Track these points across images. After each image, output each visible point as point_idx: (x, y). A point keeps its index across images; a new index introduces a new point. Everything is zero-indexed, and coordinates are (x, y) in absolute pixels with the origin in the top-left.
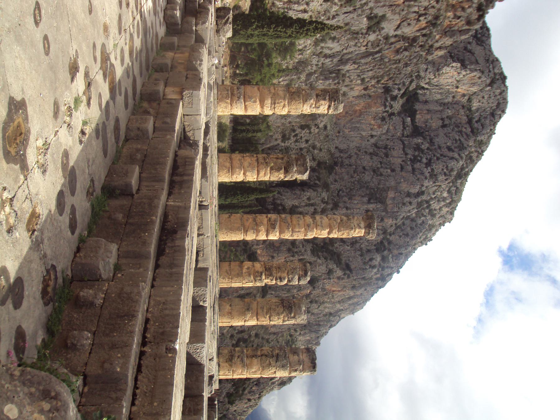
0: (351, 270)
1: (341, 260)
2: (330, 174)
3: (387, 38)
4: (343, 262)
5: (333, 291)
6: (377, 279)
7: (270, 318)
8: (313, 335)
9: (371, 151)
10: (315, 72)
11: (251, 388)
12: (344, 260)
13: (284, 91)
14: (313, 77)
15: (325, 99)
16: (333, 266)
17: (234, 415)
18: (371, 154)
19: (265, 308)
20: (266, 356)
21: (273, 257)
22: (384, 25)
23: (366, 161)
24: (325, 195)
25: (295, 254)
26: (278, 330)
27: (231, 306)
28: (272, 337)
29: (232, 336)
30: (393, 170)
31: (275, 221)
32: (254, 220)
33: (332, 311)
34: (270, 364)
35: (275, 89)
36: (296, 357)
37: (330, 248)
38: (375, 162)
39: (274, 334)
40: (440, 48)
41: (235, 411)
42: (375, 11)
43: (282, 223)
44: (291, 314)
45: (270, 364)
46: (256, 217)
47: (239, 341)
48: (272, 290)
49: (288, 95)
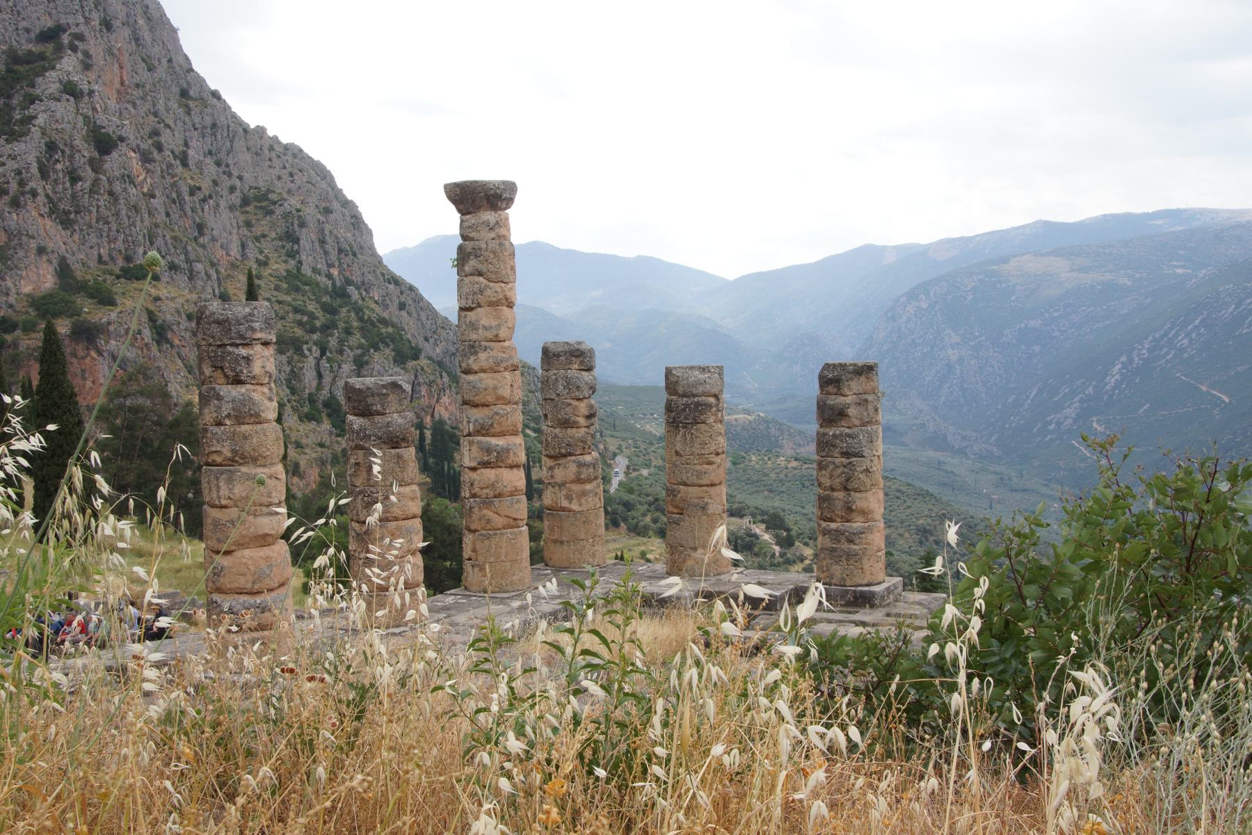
1: (30, 52)
4: (36, 48)
5: (122, 84)
7: (718, 454)
8: (240, 144)
11: (376, 302)
13: (230, 481)
15: (248, 359)
16: (49, 83)
19: (699, 467)
20: (847, 480)
21: (41, 251)
25: (27, 188)
26: (235, 237)
27: (695, 549)
28: (252, 253)
31: (488, 450)
32: (487, 503)
33: (176, 90)
34: (867, 471)
35: (225, 507)
36: (852, 411)
39: (243, 246)
43: (492, 431)
44: (710, 406)
45: (867, 471)
46: (474, 496)
49: (244, 469)
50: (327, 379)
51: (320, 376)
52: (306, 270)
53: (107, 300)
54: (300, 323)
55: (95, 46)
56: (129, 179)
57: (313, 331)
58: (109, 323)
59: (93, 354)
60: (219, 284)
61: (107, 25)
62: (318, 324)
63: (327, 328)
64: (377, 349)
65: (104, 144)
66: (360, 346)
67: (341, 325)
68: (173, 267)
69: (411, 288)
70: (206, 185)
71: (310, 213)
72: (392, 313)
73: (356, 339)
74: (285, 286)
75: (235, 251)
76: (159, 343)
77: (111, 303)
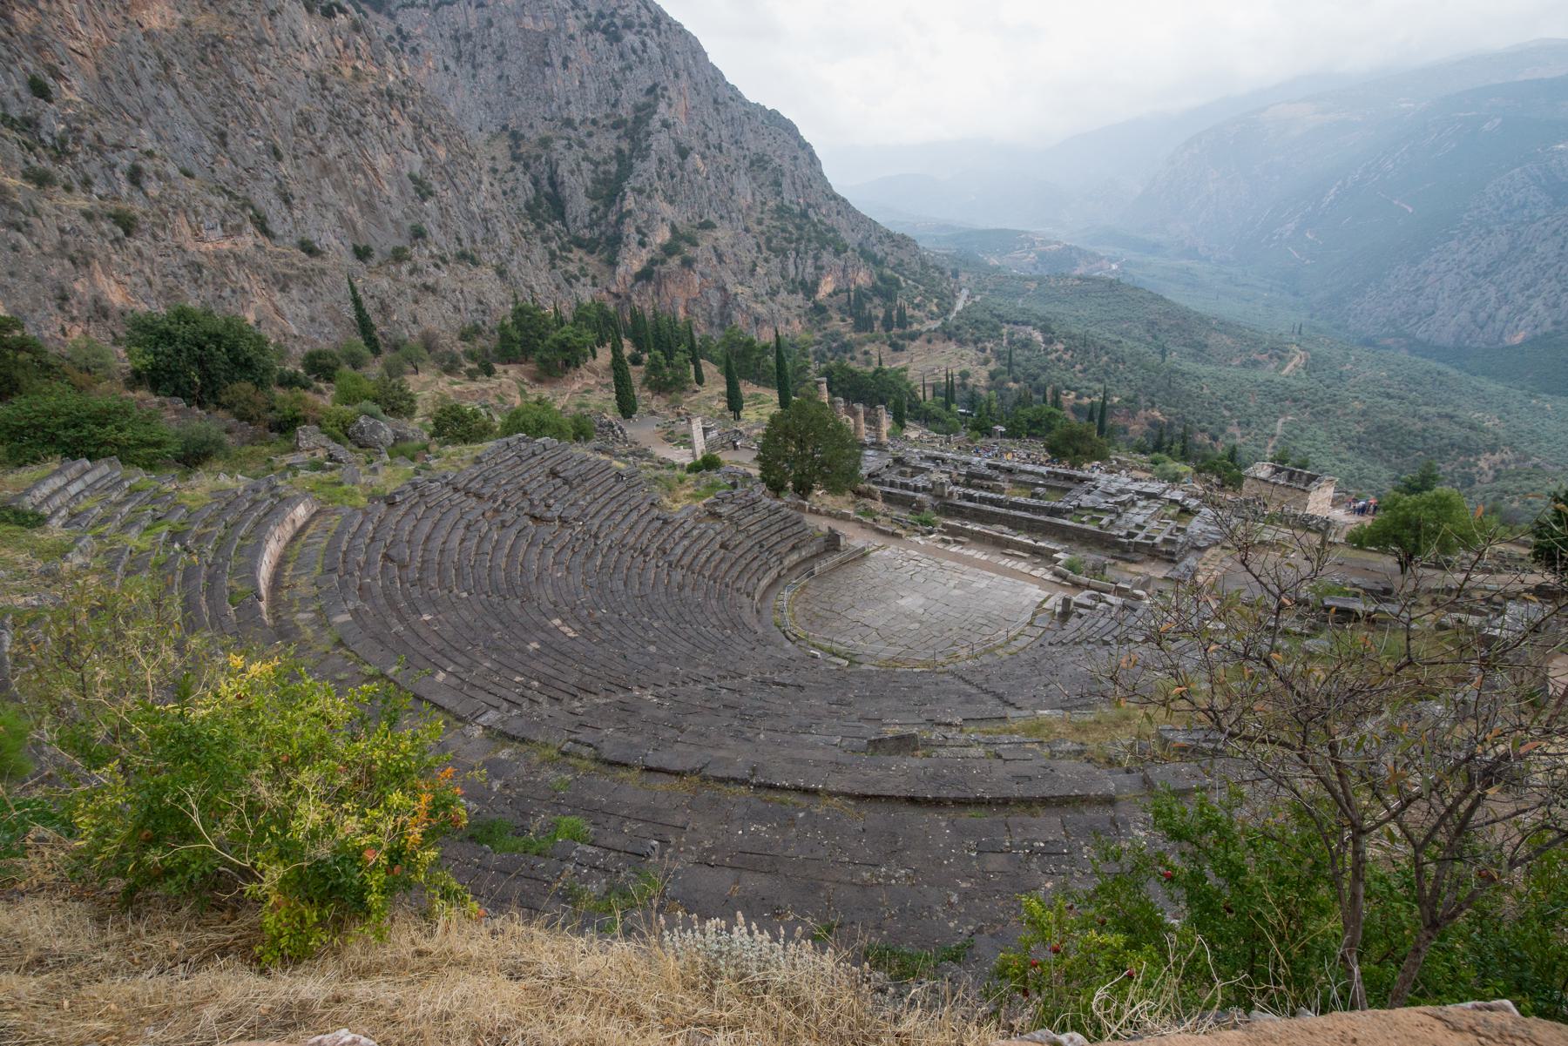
0: (655, 86)
2: (523, 136)
3: (428, 163)
6: (659, 34)
8: (747, 128)
9: (468, 67)
12: (643, 100)
16: (655, 123)
18: (474, 67)
21: (663, 220)
22: (416, 171)
23: (488, 75)
24: (559, 145)
28: (759, 198)
29: (766, 260)
30: (490, 23)
37: (630, 125)
38: (486, 57)
40: (401, 69)
42: (413, 193)
47: (769, 248)
52: (786, 202)
55: (672, 93)
56: (697, 171)
61: (677, 75)
65: (683, 153)
68: (721, 217)
69: (844, 200)
70: (732, 164)
71: (787, 165)
72: (833, 220)
73: (814, 245)
75: (749, 199)
77: (697, 245)
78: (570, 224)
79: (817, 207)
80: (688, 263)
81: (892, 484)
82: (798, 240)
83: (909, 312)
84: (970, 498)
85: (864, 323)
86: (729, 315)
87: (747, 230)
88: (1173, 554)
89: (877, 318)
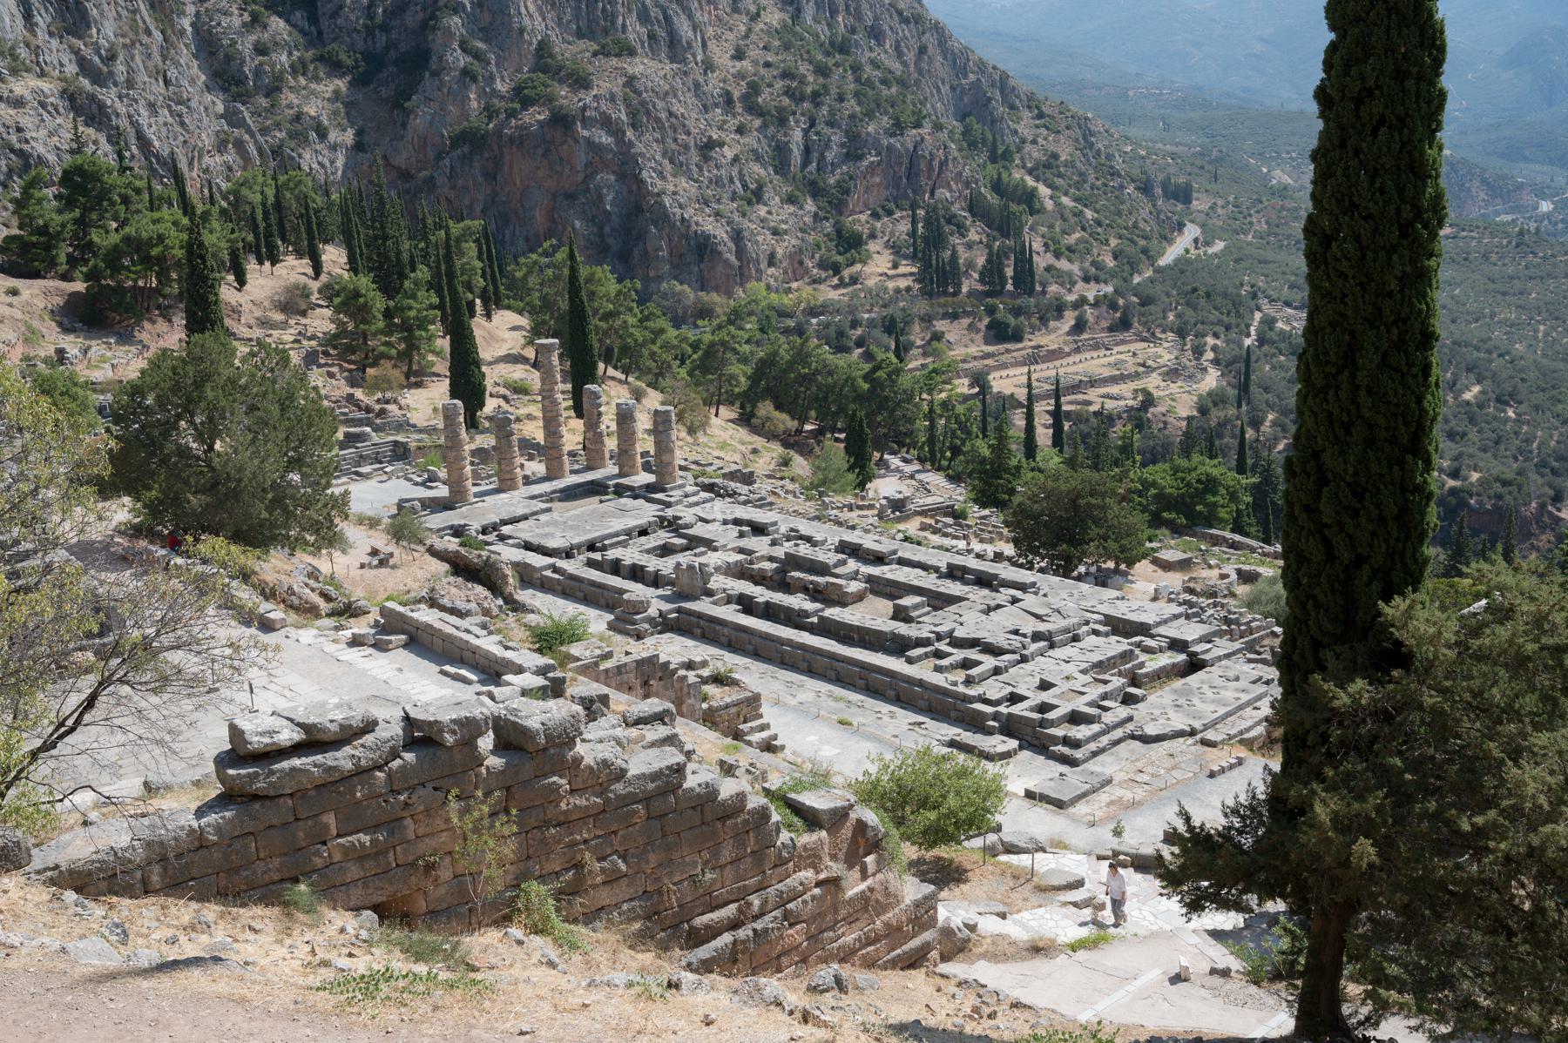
10: (77, 52)
14: (87, 52)
17: (963, 92)
29: (740, 130)
41: (953, 88)
47: (752, 108)
48: (613, 23)
50: (816, 154)
51: (807, 150)
53: (581, 82)
54: (788, 92)
57: (802, 99)
58: (584, 108)
59: (570, 140)
60: (704, 45)
62: (809, 89)
63: (816, 98)
64: (870, 115)
66: (852, 117)
67: (834, 91)
69: (937, 28)
74: (777, 43)
76: (634, 126)
78: (325, 24)
79: (876, 34)
80: (561, 121)
81: (615, 568)
82: (816, 95)
83: (1041, 261)
84: (746, 604)
85: (938, 277)
86: (642, 236)
87: (709, 67)
88: (1076, 744)
89: (971, 265)
